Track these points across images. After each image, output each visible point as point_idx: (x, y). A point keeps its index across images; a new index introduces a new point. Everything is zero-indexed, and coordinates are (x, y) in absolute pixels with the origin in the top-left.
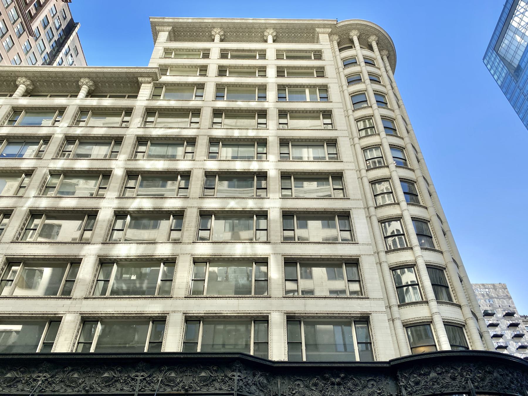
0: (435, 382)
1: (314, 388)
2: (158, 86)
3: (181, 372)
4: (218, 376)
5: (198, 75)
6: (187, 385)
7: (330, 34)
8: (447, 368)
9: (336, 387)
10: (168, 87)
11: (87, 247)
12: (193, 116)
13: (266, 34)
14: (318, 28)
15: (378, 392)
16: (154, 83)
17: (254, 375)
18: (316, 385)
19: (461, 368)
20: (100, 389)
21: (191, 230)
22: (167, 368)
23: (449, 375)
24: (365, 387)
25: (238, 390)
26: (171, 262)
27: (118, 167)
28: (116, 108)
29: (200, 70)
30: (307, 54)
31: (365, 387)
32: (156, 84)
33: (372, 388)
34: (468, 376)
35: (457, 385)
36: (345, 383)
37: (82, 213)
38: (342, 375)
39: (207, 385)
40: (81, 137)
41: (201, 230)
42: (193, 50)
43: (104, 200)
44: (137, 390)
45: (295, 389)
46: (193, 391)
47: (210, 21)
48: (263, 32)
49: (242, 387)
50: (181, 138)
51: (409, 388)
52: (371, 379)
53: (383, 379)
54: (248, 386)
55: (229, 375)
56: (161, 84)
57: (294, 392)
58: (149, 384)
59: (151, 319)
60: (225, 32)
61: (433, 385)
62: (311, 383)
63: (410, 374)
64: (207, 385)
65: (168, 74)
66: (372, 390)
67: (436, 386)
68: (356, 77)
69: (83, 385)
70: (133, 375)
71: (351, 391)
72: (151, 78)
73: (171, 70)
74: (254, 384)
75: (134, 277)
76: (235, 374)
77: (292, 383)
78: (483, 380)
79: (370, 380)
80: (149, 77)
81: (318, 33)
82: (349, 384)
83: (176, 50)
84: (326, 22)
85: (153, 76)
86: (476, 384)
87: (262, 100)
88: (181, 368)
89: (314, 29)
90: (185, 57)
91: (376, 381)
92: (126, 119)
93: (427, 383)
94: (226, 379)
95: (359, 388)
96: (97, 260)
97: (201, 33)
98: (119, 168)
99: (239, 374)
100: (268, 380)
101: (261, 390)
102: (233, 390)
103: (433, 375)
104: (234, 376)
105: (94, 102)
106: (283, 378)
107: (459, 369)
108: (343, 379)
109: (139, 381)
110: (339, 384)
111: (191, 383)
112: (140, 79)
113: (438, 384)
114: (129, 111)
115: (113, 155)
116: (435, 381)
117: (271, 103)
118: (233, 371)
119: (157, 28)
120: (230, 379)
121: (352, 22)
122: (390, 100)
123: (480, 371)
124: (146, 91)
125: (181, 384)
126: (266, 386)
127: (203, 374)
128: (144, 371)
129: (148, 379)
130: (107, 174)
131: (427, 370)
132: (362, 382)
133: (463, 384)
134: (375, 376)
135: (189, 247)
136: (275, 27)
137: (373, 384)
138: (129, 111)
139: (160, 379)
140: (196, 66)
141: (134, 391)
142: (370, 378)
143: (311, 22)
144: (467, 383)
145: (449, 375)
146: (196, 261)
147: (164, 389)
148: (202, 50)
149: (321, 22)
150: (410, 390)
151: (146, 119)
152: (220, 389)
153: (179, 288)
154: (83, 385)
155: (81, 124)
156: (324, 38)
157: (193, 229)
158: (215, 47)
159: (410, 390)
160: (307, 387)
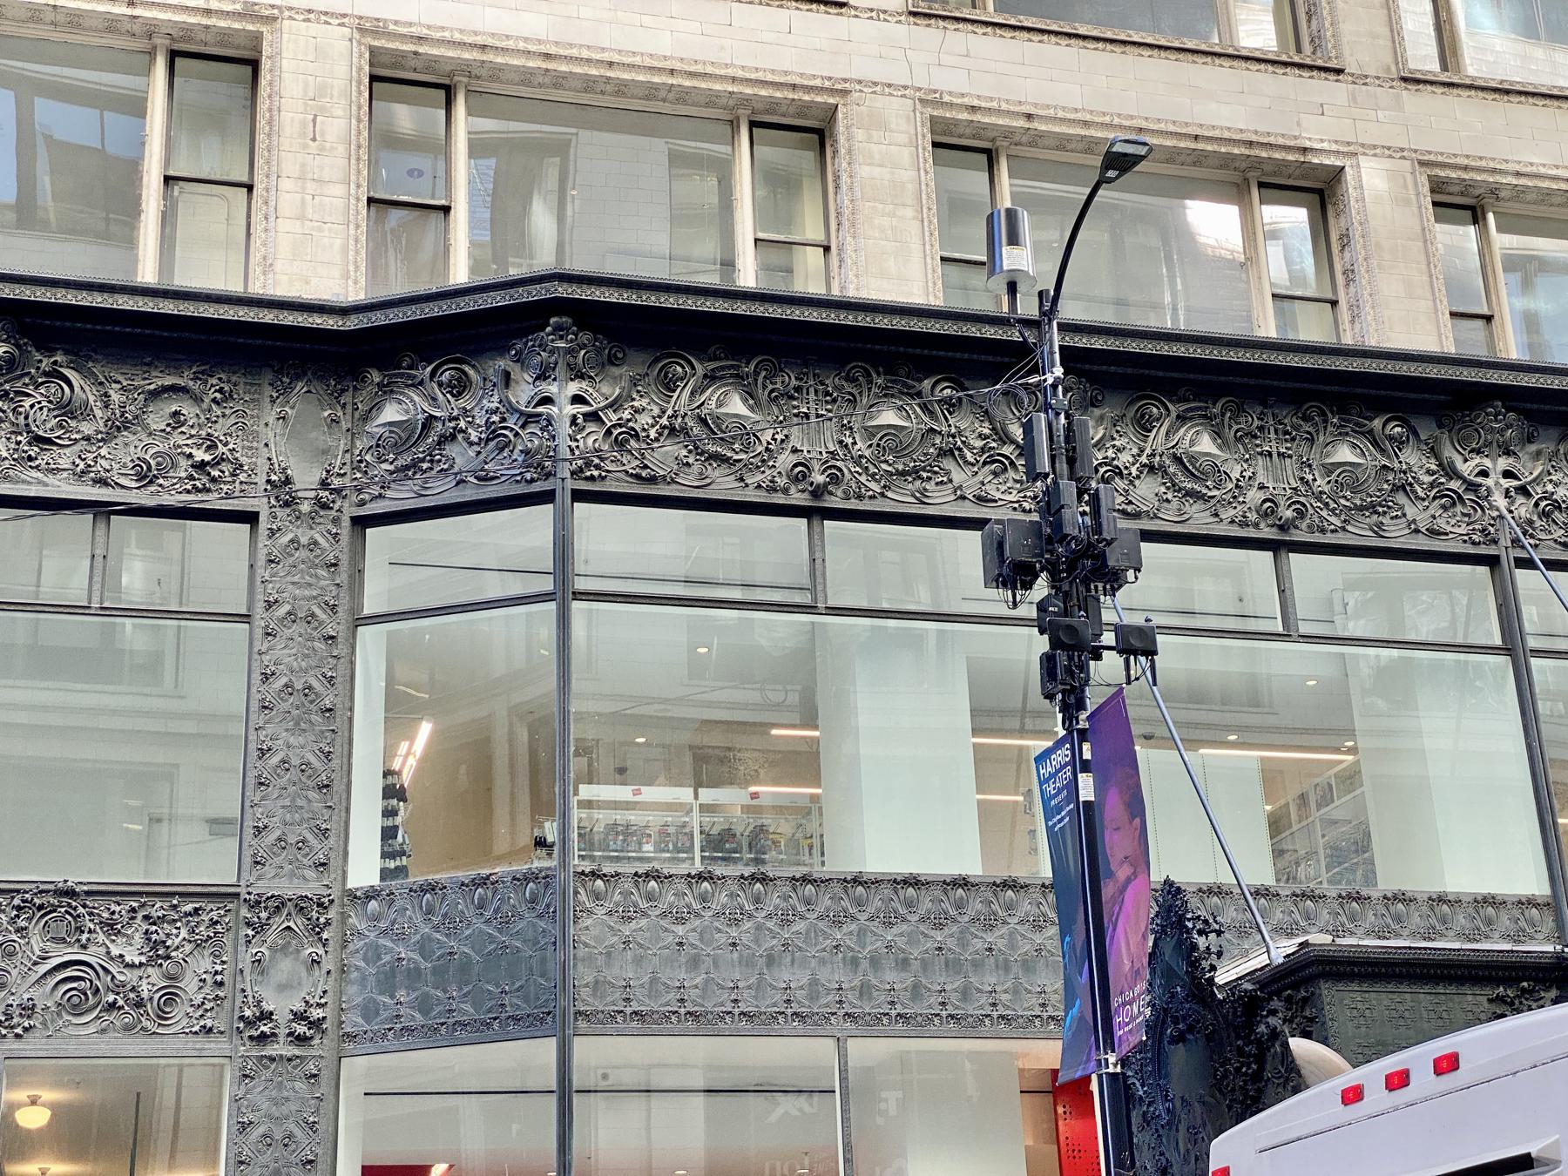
15: (201, 455)
24: (125, 426)
31: (118, 426)
52: (174, 389)
66: (162, 447)
132: (116, 397)
142: (169, 381)
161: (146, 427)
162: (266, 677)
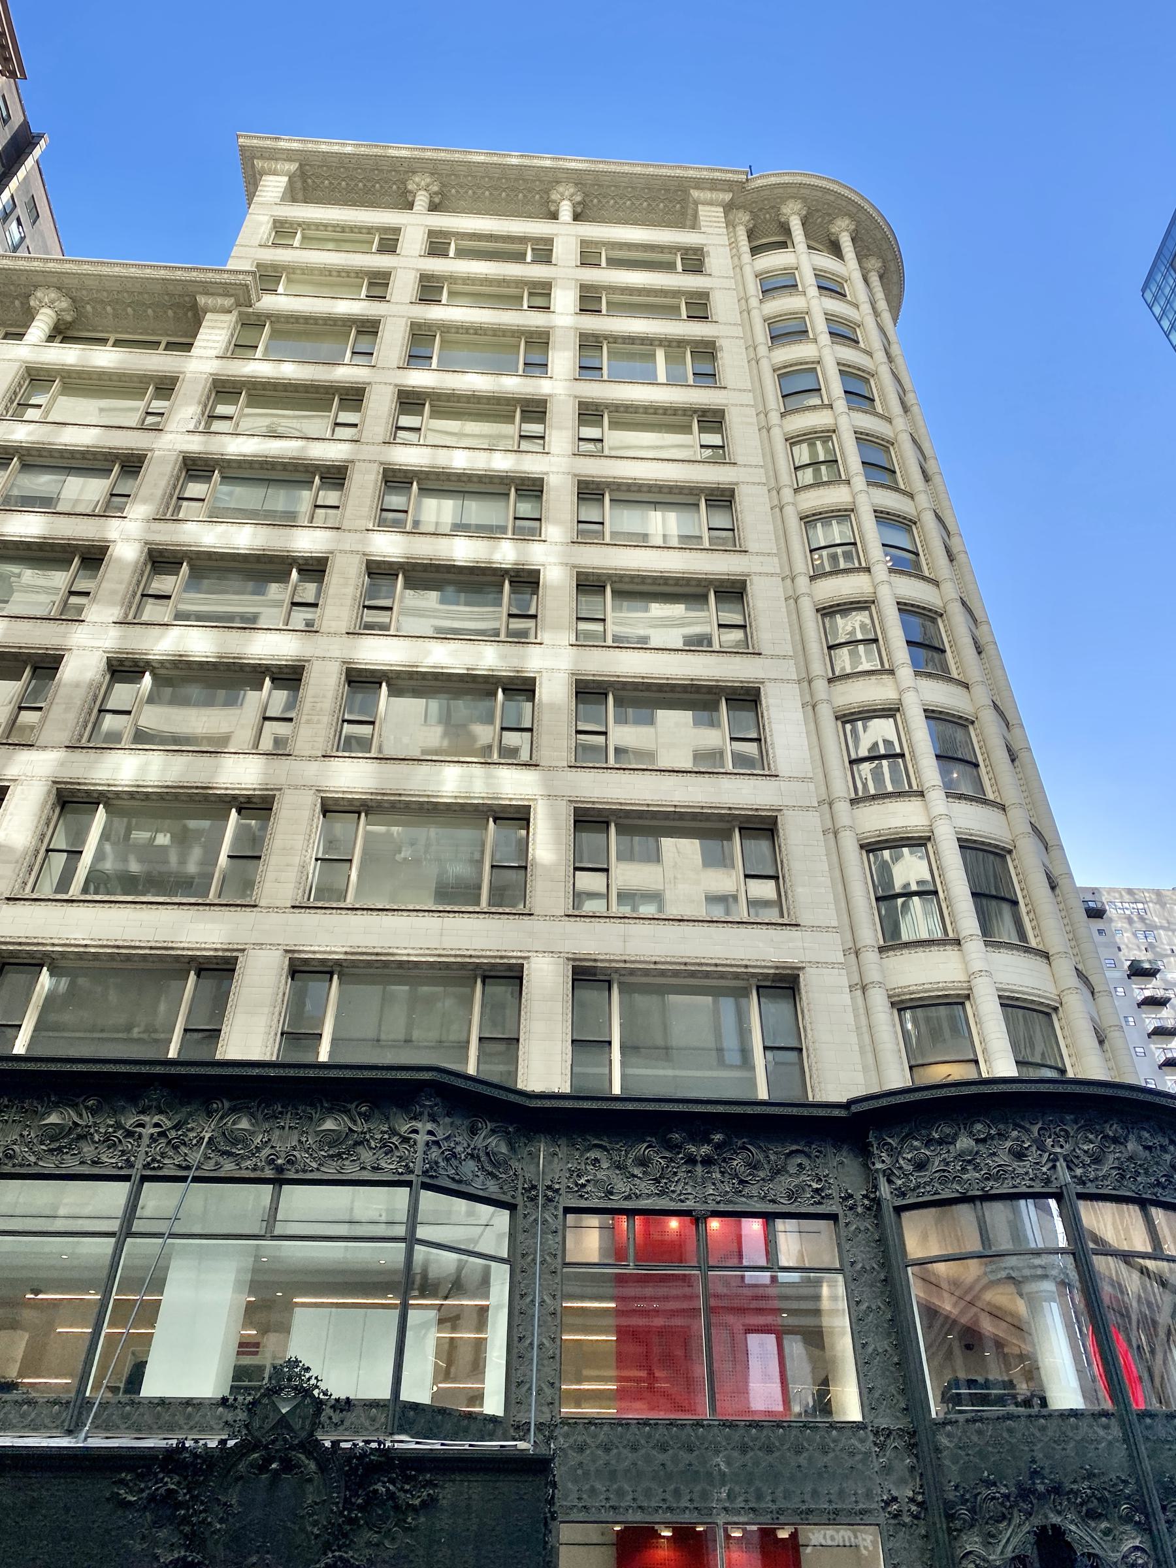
0: (969, 1162)
1: (637, 1171)
2: (251, 323)
3: (266, 1118)
4: (370, 1130)
5: (363, 296)
6: (283, 1155)
7: (728, 208)
8: (1001, 1126)
9: (699, 1169)
10: (278, 326)
11: (25, 756)
12: (341, 408)
13: (554, 196)
14: (697, 188)
15: (815, 1186)
16: (240, 313)
17: (473, 1131)
18: (643, 1162)
19: (1040, 1125)
20: (33, 1159)
22: (227, 1105)
23: (1008, 1144)
24: (778, 1172)
25: (425, 1173)
27: (126, 539)
28: (131, 376)
29: (370, 284)
30: (666, 257)
31: (777, 1172)
32: (248, 314)
33: (798, 1175)
34: (1059, 1150)
35: (1027, 1173)
36: (724, 1160)
37: (17, 660)
38: (718, 1137)
39: (339, 1155)
40: (28, 449)
42: (352, 229)
43: (81, 628)
44: (138, 1165)
45: (587, 1173)
46: (297, 1172)
47: (404, 153)
48: (547, 192)
49: (436, 1163)
50: (306, 466)
51: (899, 1178)
52: (797, 1151)
53: (830, 1150)
54: (454, 1162)
55: (404, 1129)
56: (258, 315)
57: (582, 1181)
58: (175, 1148)
60: (443, 185)
61: (964, 1170)
62: (632, 1155)
63: (902, 1140)
64: (339, 1155)
65: (281, 290)
66: (797, 1182)
67: (972, 1175)
68: (793, 326)
70: (129, 1121)
71: (741, 1182)
72: (232, 300)
73: (289, 280)
74: (472, 1156)
75: (163, 839)
76: (418, 1125)
78: (1097, 1160)
79: (792, 1152)
80: (226, 295)
81: (696, 203)
82: (737, 1163)
83: (306, 225)
84: (717, 175)
85: (238, 296)
86: (1079, 1172)
87: (537, 371)
88: (268, 1106)
89: (686, 191)
90: (331, 246)
91: (808, 1156)
92: (158, 405)
93: (947, 1164)
94: (394, 1140)
95: (762, 1174)
96: (49, 792)
97: (382, 184)
98: (128, 540)
100: (512, 1149)
101: (490, 1174)
102: (412, 1172)
103: (964, 1143)
104: (416, 1132)
105: (69, 355)
106: (555, 1142)
107: (1035, 1129)
108: (718, 1147)
109: (146, 1140)
110: (707, 1162)
112: (202, 300)
113: (977, 1168)
114: (166, 386)
115: (114, 504)
116: (969, 1160)
117: (559, 383)
118: (415, 1118)
119: (258, 164)
120: (405, 1140)
121: (787, 179)
122: (881, 390)
123: (1091, 1136)
124: (214, 335)
125: (266, 1152)
127: (329, 1125)
129: (172, 1134)
130: (93, 557)
131: (947, 1130)
132: (772, 1157)
133: (1044, 1169)
134: (809, 1144)
136: (578, 179)
137: (800, 1165)
138: (166, 386)
139: (208, 1136)
140: (359, 274)
141: (132, 1166)
142: (794, 1147)
143: (679, 172)
144: (1054, 1167)
145: (1008, 1144)
147: (217, 1164)
148: (378, 229)
149: (705, 174)
150: (899, 1182)
151: (213, 408)
152: (376, 1169)
155: (31, 414)
156: (711, 217)
158: (415, 225)
159: (899, 1182)
160: (618, 1167)
161: (787, 1172)
162: (858, 1303)
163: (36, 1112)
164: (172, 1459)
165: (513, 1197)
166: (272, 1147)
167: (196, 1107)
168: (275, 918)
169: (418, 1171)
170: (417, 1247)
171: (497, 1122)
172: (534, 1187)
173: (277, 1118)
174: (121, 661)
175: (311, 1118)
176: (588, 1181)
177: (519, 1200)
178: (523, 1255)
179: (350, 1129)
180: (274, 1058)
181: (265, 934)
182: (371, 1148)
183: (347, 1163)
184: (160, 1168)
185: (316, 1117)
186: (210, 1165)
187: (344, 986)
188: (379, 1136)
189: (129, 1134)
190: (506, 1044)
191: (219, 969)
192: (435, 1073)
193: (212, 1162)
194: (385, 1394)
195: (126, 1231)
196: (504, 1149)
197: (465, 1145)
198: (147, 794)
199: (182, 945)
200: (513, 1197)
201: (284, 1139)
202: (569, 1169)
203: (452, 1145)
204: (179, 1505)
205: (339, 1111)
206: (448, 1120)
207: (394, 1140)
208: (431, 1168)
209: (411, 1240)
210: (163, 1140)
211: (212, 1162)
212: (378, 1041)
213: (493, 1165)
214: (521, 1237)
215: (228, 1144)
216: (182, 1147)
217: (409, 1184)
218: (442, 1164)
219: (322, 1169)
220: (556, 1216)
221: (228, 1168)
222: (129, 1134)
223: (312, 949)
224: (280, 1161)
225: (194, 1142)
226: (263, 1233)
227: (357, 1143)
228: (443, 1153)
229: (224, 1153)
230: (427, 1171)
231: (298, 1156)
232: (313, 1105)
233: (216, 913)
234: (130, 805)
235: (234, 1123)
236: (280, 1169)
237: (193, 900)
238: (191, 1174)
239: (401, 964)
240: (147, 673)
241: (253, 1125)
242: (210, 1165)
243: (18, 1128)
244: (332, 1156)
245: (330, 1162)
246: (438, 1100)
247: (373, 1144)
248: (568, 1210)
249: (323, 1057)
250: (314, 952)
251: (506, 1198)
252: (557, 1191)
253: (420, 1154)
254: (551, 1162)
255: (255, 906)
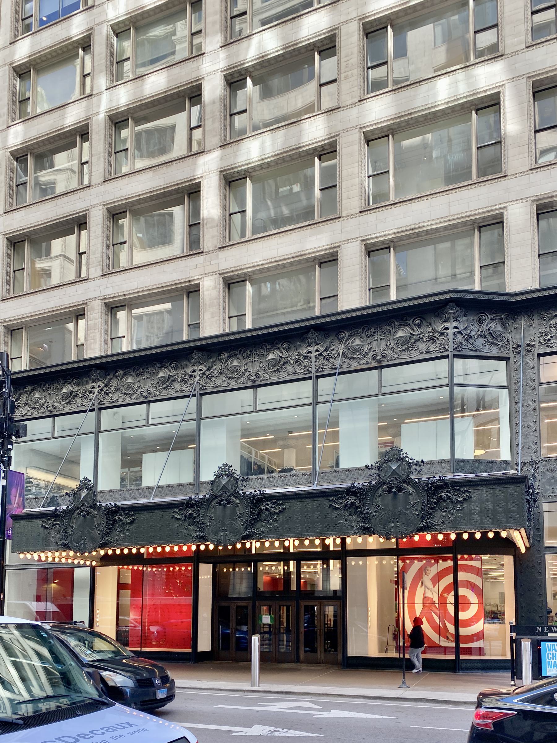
3: (368, 337)
4: (422, 333)
6: (379, 354)
21: (352, 75)
22: (347, 334)
25: (455, 349)
26: (328, 151)
39: (408, 349)
41: (373, 67)
44: (313, 371)
46: (388, 361)
49: (461, 343)
54: (471, 341)
57: (549, 337)
58: (328, 360)
59: (317, 261)
64: (408, 349)
69: (247, 374)
70: (304, 351)
74: (481, 336)
76: (448, 324)
77: (544, 323)
88: (367, 330)
94: (436, 335)
99: (455, 324)
100: (505, 328)
104: (447, 328)
106: (530, 318)
109: (314, 359)
111: (384, 349)
118: (446, 321)
120: (442, 334)
126: (501, 335)
128: (318, 344)
129: (325, 354)
135: (354, 112)
139: (341, 351)
141: (311, 372)
146: (372, 138)
147: (349, 364)
152: (428, 352)
153: (348, 198)
154: (247, 374)
157: (356, 71)
163: (263, 355)
164: (351, 491)
165: (507, 353)
166: (374, 351)
167: (333, 338)
168: (352, 222)
169: (451, 349)
170: (455, 388)
171: (493, 314)
172: (519, 346)
173: (373, 335)
174: (231, 74)
175: (390, 332)
176: (552, 337)
177: (511, 355)
178: (516, 383)
179: (411, 334)
180: (368, 304)
181: (346, 234)
182: (424, 342)
183: (412, 352)
184: (323, 371)
185: (393, 331)
186: (345, 365)
187: (397, 254)
188: (427, 335)
189: (306, 357)
190: (497, 266)
191: (329, 260)
192: (453, 294)
193: (346, 364)
194: (448, 456)
195: (316, 403)
196: (499, 328)
197: (477, 330)
198: (268, 163)
199: (308, 252)
200: (507, 353)
201: (378, 345)
202: (540, 333)
203: (469, 332)
204: (357, 507)
205: (405, 325)
206: (465, 318)
207: (436, 335)
208: (458, 346)
209: (452, 385)
210: (322, 358)
211: (346, 364)
212: (436, 279)
213: (493, 338)
214: (513, 374)
215: (352, 354)
216: (331, 359)
217: (447, 357)
218: (464, 343)
219: (400, 357)
220: (533, 360)
221: (355, 365)
222: (306, 357)
223: (376, 235)
224: (378, 358)
225: (336, 355)
226: (377, 393)
227: (416, 341)
228: (464, 337)
229: (350, 359)
230: (456, 348)
231: (387, 353)
232: (389, 325)
233: (322, 227)
234: (260, 173)
235: (352, 343)
236: (379, 361)
237: (307, 223)
238: (337, 371)
239: (427, 232)
240: (248, 78)
241: (362, 342)
242: (345, 365)
243: (258, 364)
244: (404, 350)
245: (403, 353)
246: (458, 309)
247: (425, 340)
248: (540, 355)
249: (393, 298)
250: (377, 237)
251: (504, 355)
252: (533, 346)
253: (451, 340)
254: (528, 330)
255: (340, 217)
